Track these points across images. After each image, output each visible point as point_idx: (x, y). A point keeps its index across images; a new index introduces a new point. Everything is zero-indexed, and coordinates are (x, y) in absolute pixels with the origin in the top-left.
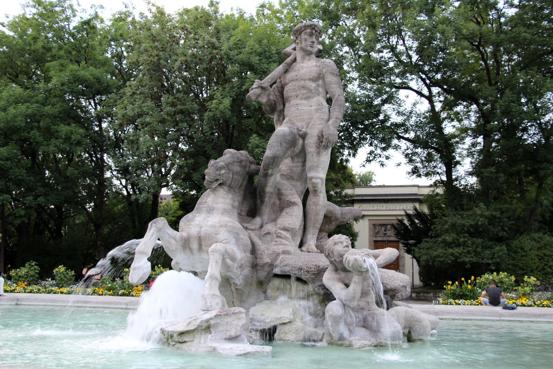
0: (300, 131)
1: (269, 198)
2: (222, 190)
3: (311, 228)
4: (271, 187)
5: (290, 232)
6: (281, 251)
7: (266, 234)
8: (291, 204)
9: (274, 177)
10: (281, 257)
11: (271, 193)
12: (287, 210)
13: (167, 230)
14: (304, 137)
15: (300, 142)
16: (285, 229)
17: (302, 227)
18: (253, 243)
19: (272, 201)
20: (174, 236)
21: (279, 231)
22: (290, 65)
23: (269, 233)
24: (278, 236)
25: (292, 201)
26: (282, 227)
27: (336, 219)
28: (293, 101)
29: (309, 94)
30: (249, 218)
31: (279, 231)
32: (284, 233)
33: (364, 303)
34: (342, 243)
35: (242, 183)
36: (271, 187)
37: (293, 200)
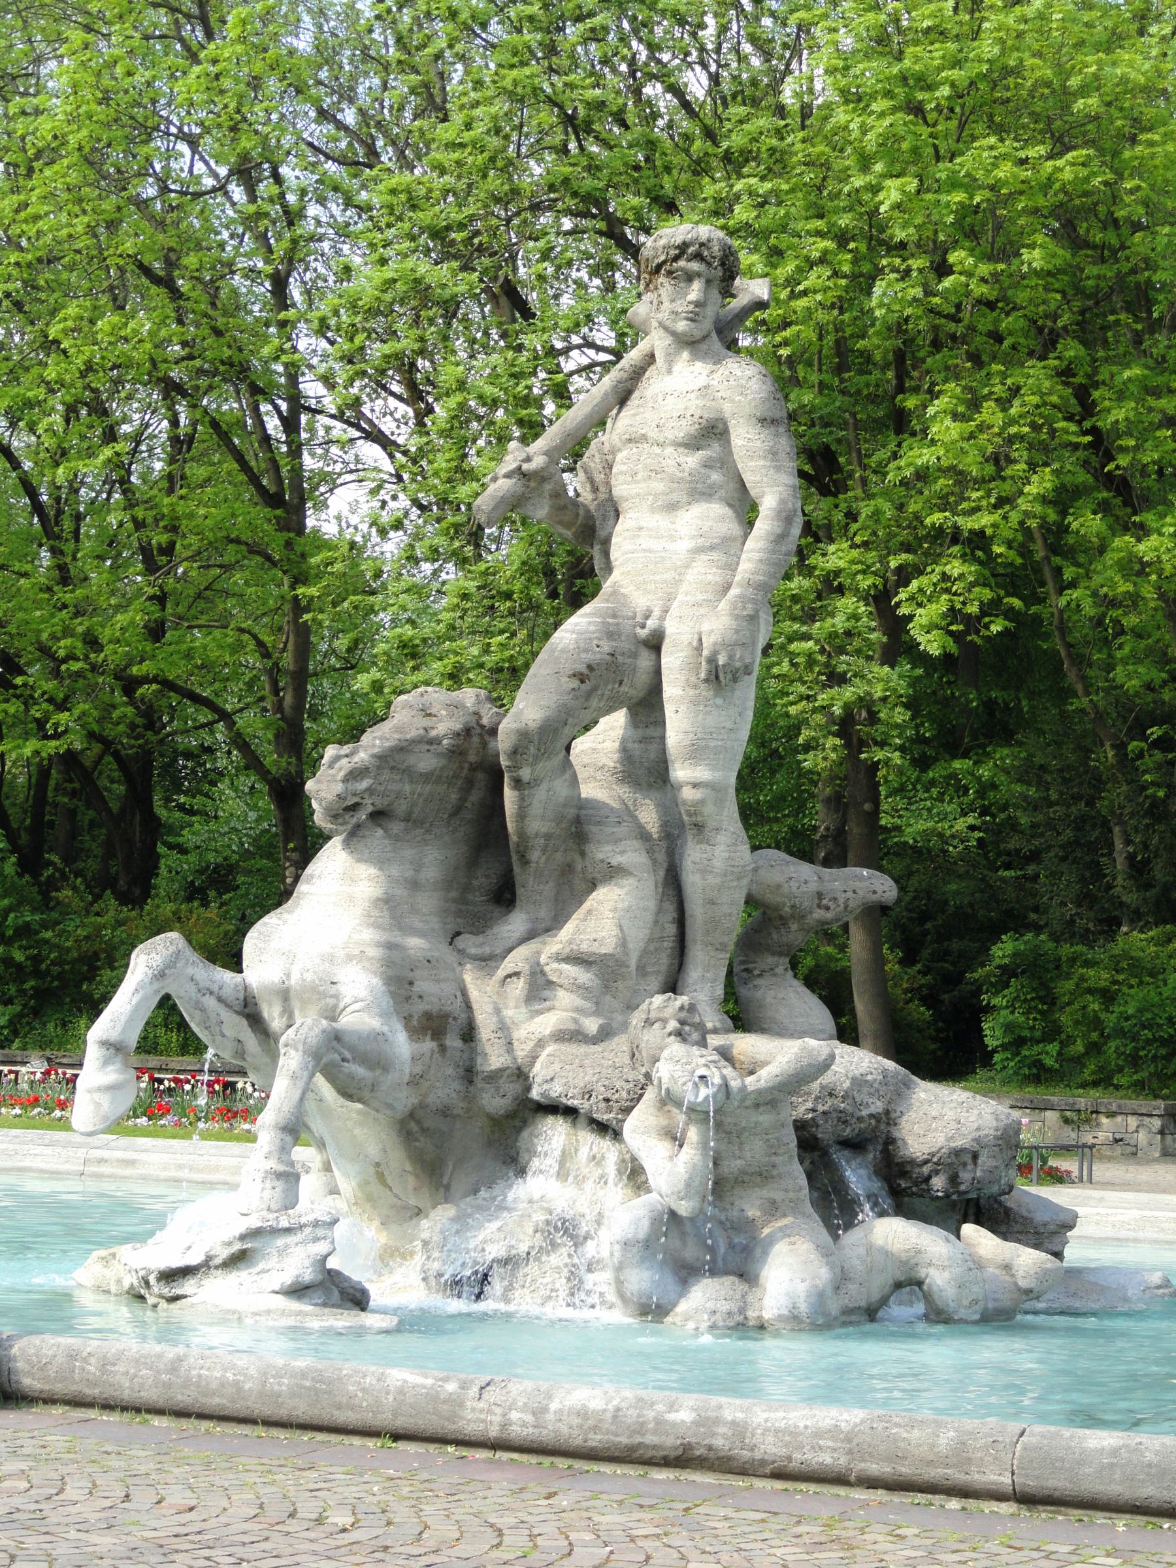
1: (544, 851)
2: (380, 832)
3: (699, 946)
4: (543, 817)
5: (594, 968)
6: (547, 1032)
7: (509, 976)
9: (544, 786)
10: (550, 1049)
11: (548, 837)
13: (190, 970)
14: (655, 644)
15: (645, 661)
17: (669, 944)
19: (559, 856)
20: (215, 988)
22: (638, 374)
25: (614, 862)
26: (567, 950)
27: (799, 915)
28: (630, 514)
30: (497, 911)
31: (555, 965)
35: (463, 799)
36: (543, 817)
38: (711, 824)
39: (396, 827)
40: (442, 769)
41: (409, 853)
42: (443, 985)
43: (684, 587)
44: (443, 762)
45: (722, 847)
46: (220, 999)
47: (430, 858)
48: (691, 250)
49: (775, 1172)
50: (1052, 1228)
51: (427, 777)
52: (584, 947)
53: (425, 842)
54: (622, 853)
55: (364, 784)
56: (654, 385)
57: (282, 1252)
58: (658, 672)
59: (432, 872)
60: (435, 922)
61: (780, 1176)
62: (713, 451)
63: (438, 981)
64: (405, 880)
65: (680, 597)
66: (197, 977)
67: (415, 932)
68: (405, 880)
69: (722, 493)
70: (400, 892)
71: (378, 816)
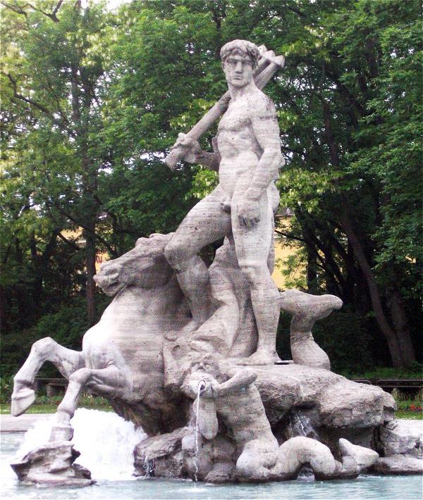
0: (222, 204)
2: (131, 293)
8: (219, 304)
12: (218, 312)
15: (225, 218)
18: (163, 361)
21: (193, 342)
23: (178, 346)
24: (192, 349)
25: (219, 299)
29: (233, 151)
31: (193, 342)
32: (199, 343)
33: (246, 433)
34: (199, 363)
37: (220, 298)
39: (137, 290)
40: (154, 266)
41: (141, 301)
43: (236, 188)
44: (152, 264)
45: (262, 291)
46: (69, 362)
48: (234, 51)
49: (251, 420)
51: (146, 270)
52: (205, 334)
53: (151, 296)
54: (222, 295)
56: (232, 105)
57: (54, 457)
58: (230, 222)
61: (254, 422)
62: (246, 131)
63: (150, 350)
64: (140, 312)
65: (236, 192)
68: (140, 312)
69: (251, 148)
70: (137, 316)
71: (131, 286)
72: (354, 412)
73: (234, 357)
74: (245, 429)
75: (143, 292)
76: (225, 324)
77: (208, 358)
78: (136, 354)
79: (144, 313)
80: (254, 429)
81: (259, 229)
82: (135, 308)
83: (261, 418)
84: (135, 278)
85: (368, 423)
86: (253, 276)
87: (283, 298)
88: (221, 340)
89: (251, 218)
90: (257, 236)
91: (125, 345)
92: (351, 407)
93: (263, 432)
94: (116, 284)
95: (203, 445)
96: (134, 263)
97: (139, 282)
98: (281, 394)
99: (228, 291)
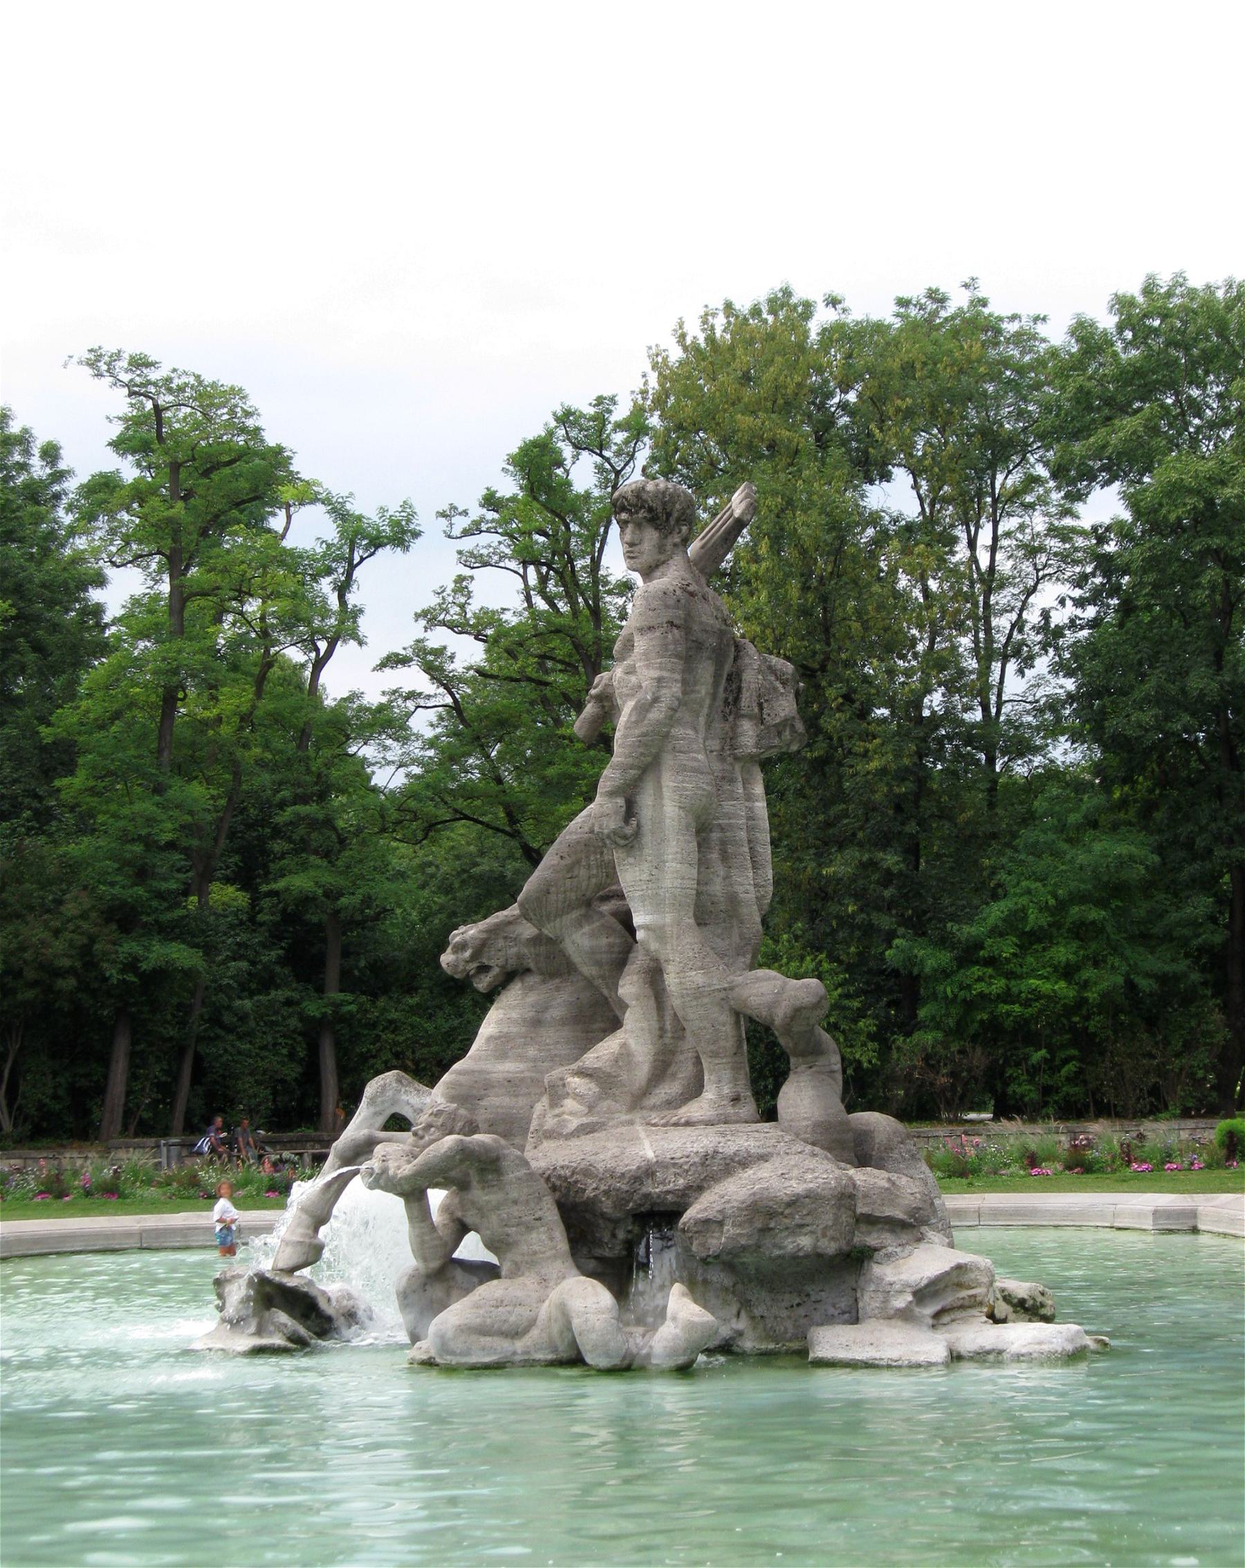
11: (603, 977)
13: (404, 1097)
16: (581, 1073)
38: (662, 958)
41: (532, 998)
42: (520, 1098)
47: (559, 1001)
50: (897, 1287)
53: (558, 989)
55: (467, 954)
59: (556, 1013)
60: (563, 1050)
61: (516, 1243)
63: (516, 1096)
64: (524, 1020)
66: (411, 1101)
67: (521, 1058)
72: (726, 1228)
73: (653, 1108)
74: (509, 1256)
75: (544, 982)
76: (632, 1043)
77: (436, 1115)
78: (482, 1103)
79: (536, 1023)
80: (518, 1258)
81: (647, 851)
82: (514, 1015)
83: (534, 1235)
84: (520, 957)
85: (777, 1252)
86: (654, 946)
87: (732, 989)
88: (609, 1075)
89: (606, 831)
90: (645, 866)
91: (461, 1085)
92: (720, 1217)
93: (532, 1262)
94: (484, 969)
95: (425, 1284)
96: (511, 928)
97: (532, 966)
98: (603, 1187)
99: (635, 978)
